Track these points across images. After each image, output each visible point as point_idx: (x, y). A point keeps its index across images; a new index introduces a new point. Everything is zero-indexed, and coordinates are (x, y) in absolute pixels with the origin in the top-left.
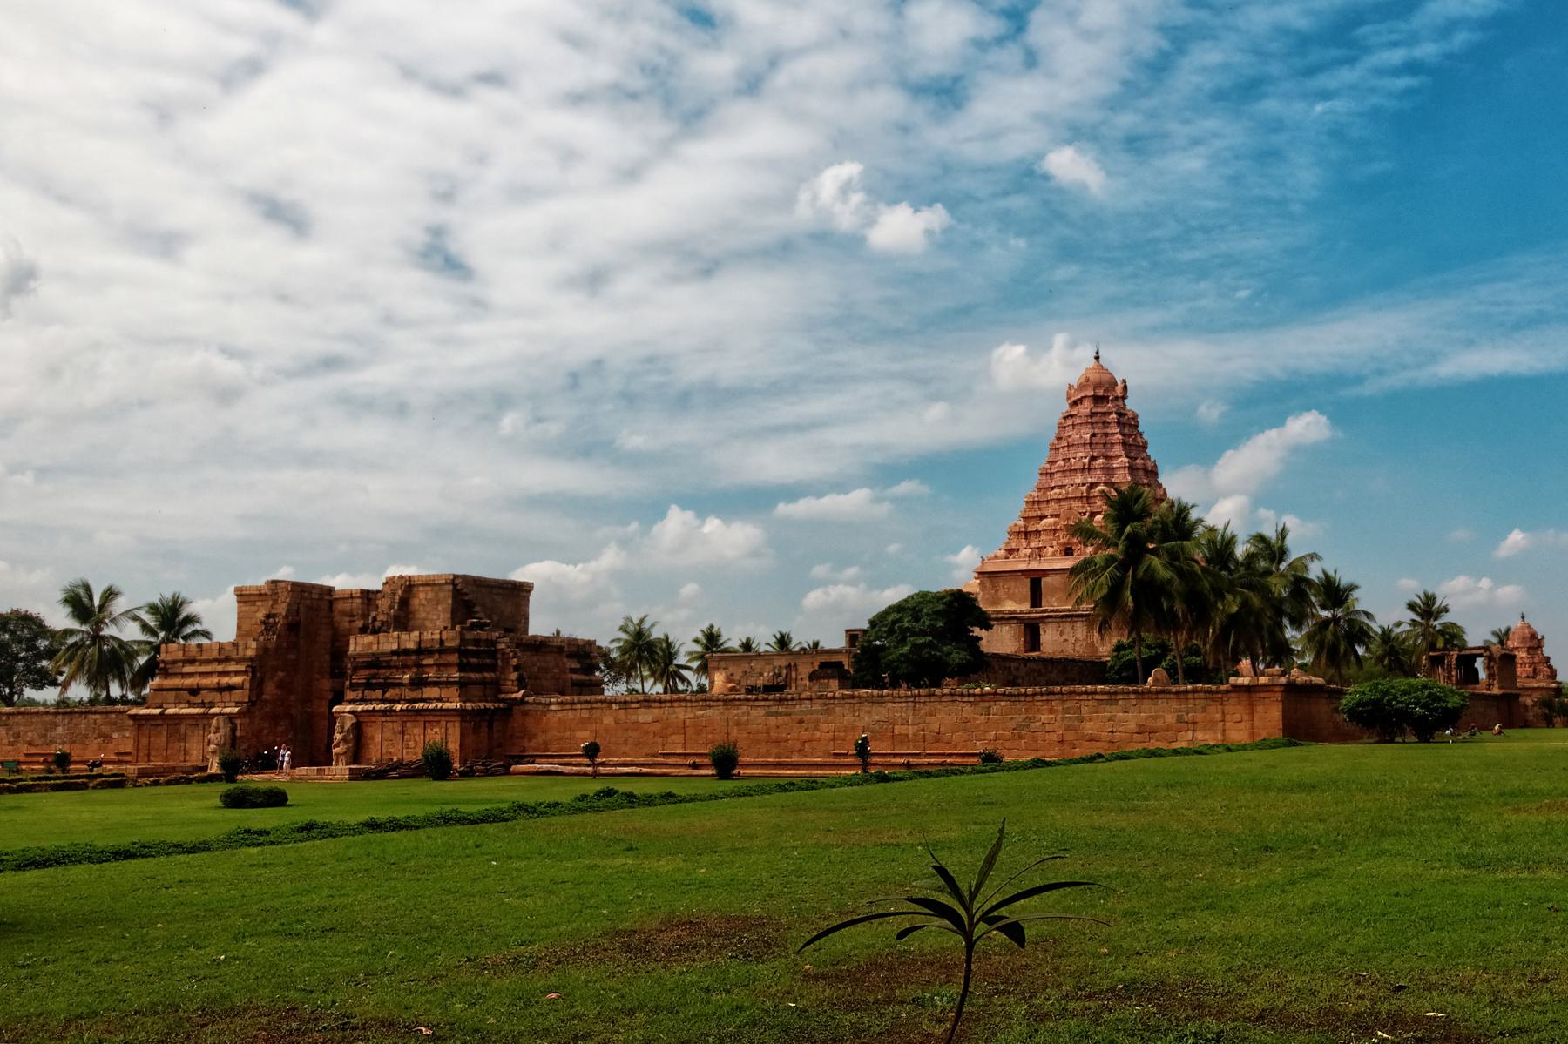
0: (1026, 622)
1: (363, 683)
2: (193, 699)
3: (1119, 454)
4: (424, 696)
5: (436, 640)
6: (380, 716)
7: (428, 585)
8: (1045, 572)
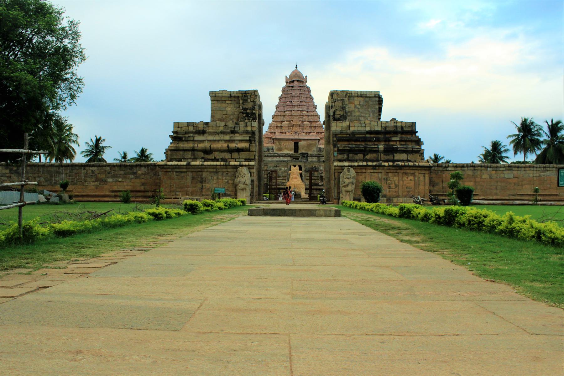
1: (347, 150)
2: (207, 156)
4: (395, 158)
5: (399, 126)
6: (370, 169)
7: (361, 96)
8: (300, 140)
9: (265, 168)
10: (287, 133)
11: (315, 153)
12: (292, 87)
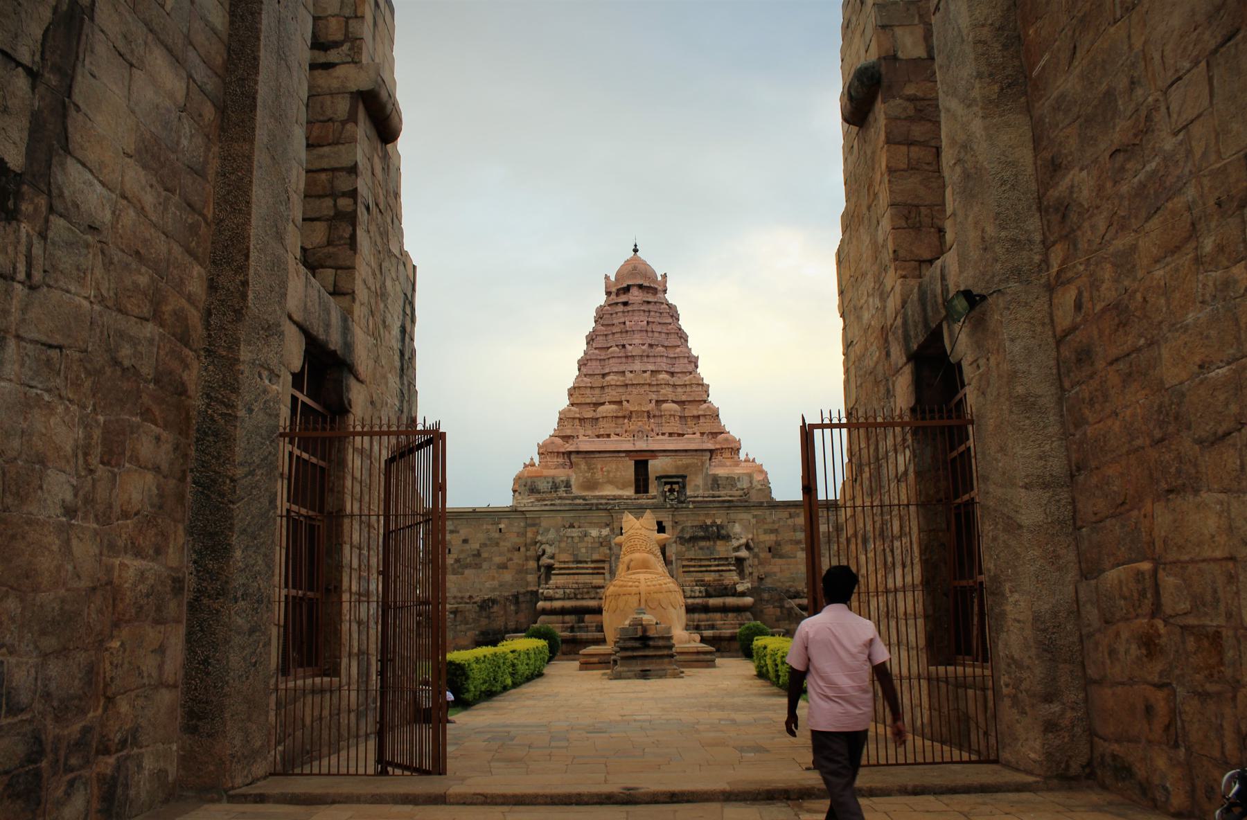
3: (675, 344)
9: (529, 535)
10: (612, 434)
11: (701, 492)
12: (625, 304)
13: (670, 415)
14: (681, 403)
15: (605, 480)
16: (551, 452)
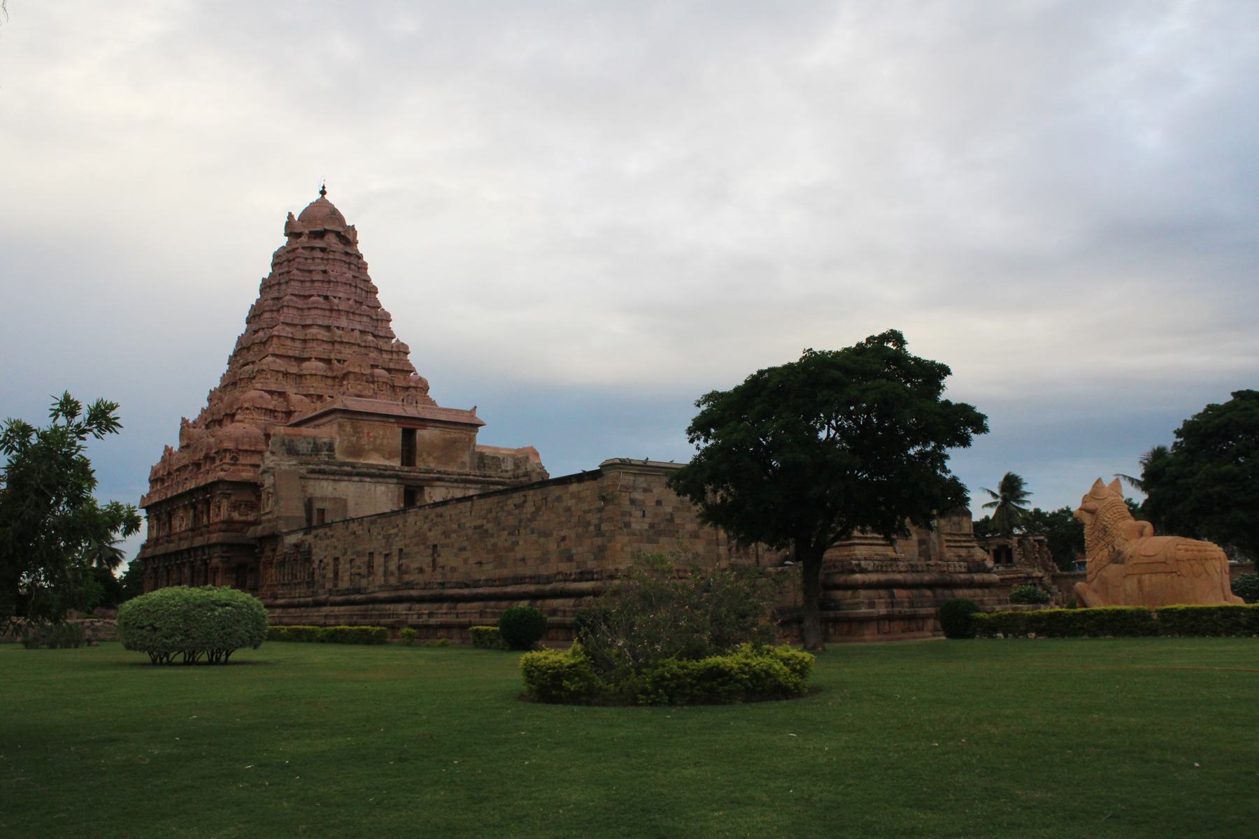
0: (409, 483)
11: (467, 470)
13: (383, 382)
14: (389, 370)
15: (371, 447)
16: (258, 408)
